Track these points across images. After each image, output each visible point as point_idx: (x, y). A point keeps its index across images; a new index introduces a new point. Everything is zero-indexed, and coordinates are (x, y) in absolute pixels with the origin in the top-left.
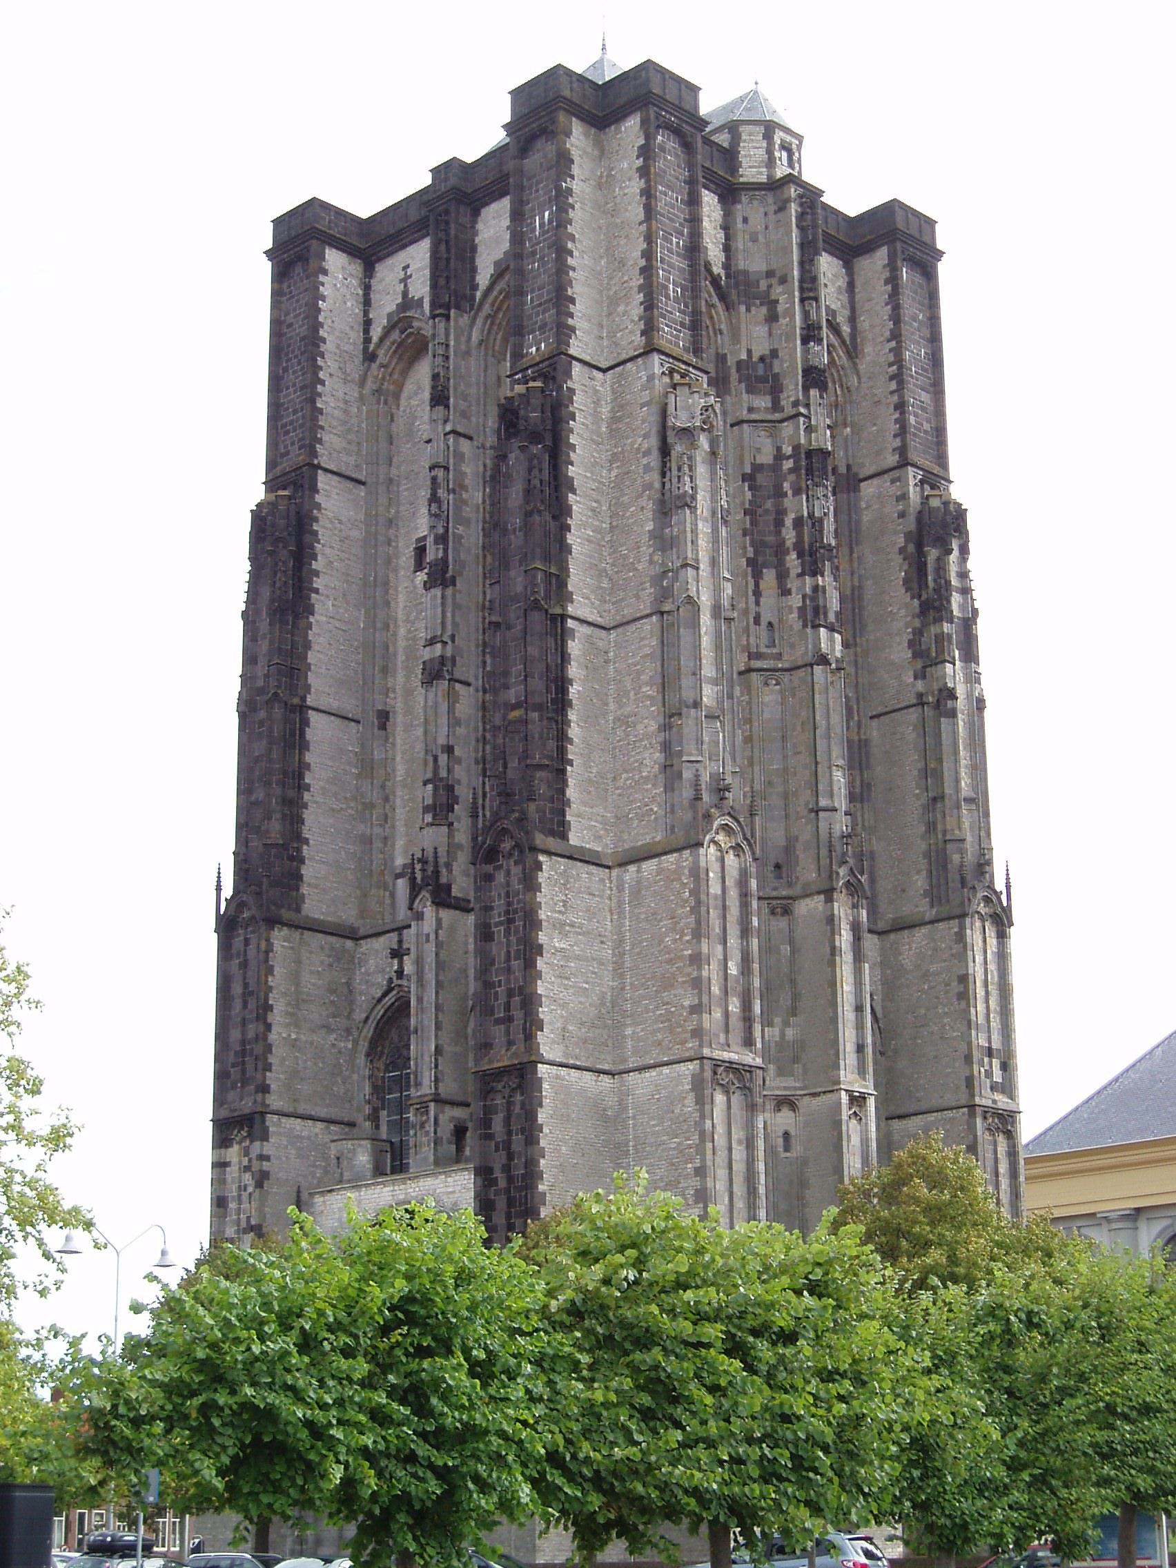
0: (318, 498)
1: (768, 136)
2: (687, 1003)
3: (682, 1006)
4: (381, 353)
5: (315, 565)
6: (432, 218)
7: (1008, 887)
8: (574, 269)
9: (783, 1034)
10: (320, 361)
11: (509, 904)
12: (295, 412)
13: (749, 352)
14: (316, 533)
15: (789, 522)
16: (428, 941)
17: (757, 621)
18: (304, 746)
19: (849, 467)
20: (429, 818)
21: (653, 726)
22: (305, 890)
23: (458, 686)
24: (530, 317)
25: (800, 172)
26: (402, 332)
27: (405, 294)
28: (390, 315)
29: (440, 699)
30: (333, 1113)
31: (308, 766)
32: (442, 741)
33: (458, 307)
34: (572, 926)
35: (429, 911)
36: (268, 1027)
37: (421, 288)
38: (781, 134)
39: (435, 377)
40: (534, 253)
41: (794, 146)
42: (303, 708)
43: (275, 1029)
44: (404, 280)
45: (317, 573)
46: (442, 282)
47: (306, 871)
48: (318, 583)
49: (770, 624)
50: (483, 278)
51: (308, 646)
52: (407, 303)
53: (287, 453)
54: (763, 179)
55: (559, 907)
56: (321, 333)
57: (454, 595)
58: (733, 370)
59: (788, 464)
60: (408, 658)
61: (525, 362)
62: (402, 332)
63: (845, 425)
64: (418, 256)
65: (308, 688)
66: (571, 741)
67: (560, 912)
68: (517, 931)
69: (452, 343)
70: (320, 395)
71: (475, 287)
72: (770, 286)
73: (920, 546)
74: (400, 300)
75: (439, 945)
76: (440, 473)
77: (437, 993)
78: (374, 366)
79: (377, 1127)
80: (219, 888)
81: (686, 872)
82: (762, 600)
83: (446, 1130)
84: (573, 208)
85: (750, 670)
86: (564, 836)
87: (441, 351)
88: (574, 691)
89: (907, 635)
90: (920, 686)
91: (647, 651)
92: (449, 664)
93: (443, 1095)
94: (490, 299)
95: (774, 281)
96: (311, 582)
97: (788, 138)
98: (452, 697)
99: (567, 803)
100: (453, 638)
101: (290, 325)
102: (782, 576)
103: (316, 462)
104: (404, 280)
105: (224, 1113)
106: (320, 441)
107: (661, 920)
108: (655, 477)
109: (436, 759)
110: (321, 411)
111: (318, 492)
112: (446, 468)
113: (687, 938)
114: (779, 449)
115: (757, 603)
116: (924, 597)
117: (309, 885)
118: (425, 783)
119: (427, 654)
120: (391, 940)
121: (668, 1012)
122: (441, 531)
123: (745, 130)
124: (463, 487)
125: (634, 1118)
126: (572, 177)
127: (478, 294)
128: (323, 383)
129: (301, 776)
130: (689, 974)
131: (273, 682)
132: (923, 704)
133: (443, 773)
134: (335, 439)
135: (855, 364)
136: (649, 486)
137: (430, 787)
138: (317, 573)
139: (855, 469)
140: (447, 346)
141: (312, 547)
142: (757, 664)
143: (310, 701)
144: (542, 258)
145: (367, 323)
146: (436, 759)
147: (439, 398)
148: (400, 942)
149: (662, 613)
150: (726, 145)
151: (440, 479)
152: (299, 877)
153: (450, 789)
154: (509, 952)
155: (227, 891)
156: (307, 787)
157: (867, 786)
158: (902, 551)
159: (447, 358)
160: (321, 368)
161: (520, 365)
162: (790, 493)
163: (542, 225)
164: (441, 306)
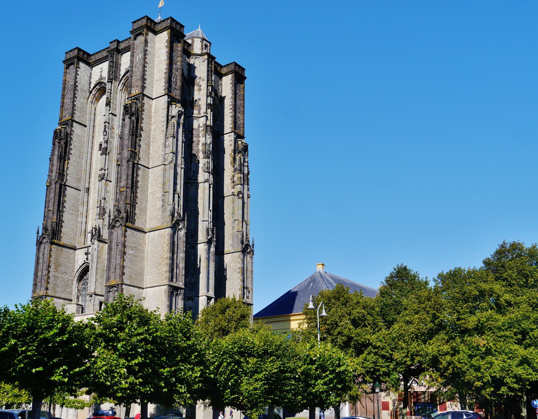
0: (73, 129)
1: (202, 42)
2: (164, 270)
4: (93, 91)
6: (109, 55)
7: (253, 245)
9: (191, 280)
11: (117, 240)
12: (68, 105)
14: (72, 138)
15: (200, 144)
16: (95, 250)
17: (190, 170)
18: (65, 196)
20: (98, 217)
22: (62, 235)
23: (108, 182)
24: (134, 83)
25: (210, 52)
27: (101, 76)
28: (96, 81)
29: (103, 185)
30: (66, 297)
31: (65, 201)
32: (103, 196)
33: (115, 80)
35: (96, 242)
36: (49, 272)
37: (105, 74)
39: (107, 98)
40: (136, 66)
42: (65, 185)
44: (101, 72)
45: (71, 149)
46: (111, 72)
47: (63, 230)
48: (71, 152)
49: (194, 171)
50: (122, 73)
51: (67, 168)
52: (101, 78)
53: (65, 116)
54: (200, 53)
57: (109, 157)
58: (188, 103)
59: (201, 129)
61: (132, 95)
64: (105, 65)
65: (67, 180)
66: (137, 198)
68: (119, 248)
69: (112, 89)
70: (75, 101)
71: (120, 75)
72: (200, 81)
73: (235, 153)
74: (99, 77)
75: (98, 251)
76: (107, 124)
77: (97, 265)
78: (91, 95)
79: (78, 301)
80: (38, 233)
81: (167, 234)
82: (192, 164)
83: (97, 303)
84: (147, 55)
86: (134, 223)
87: (110, 91)
88: (139, 184)
89: (231, 176)
90: (233, 190)
91: (160, 175)
92: (106, 176)
93: (97, 293)
94: (124, 78)
95: (201, 80)
96: (69, 151)
98: (106, 185)
99: (135, 214)
100: (108, 168)
101: (68, 82)
104: (101, 72)
105: (35, 295)
106: (75, 113)
108: (165, 128)
109: (101, 201)
110: (75, 105)
111: (73, 127)
112: (109, 123)
114: (199, 125)
115: (191, 165)
116: (235, 167)
118: (97, 207)
119: (100, 173)
120: (85, 250)
121: (159, 272)
122: (106, 140)
123: (195, 39)
124: (113, 128)
125: (148, 300)
126: (148, 47)
127: (121, 77)
128: (76, 98)
129: (63, 204)
131: (57, 178)
132: (233, 195)
133: (102, 205)
134: (79, 113)
136: (162, 131)
137: (99, 208)
138: (71, 149)
140: (111, 90)
141: (70, 142)
142: (190, 181)
143: (67, 184)
144: (138, 68)
145: (90, 83)
146: (101, 201)
147: (108, 104)
148: (88, 250)
150: (190, 43)
151: (107, 126)
152: (61, 232)
153: (104, 209)
154: (116, 254)
155: (40, 234)
156: (65, 207)
158: (230, 155)
159: (111, 93)
161: (130, 96)
162: (201, 136)
163: (139, 59)
164: (110, 79)
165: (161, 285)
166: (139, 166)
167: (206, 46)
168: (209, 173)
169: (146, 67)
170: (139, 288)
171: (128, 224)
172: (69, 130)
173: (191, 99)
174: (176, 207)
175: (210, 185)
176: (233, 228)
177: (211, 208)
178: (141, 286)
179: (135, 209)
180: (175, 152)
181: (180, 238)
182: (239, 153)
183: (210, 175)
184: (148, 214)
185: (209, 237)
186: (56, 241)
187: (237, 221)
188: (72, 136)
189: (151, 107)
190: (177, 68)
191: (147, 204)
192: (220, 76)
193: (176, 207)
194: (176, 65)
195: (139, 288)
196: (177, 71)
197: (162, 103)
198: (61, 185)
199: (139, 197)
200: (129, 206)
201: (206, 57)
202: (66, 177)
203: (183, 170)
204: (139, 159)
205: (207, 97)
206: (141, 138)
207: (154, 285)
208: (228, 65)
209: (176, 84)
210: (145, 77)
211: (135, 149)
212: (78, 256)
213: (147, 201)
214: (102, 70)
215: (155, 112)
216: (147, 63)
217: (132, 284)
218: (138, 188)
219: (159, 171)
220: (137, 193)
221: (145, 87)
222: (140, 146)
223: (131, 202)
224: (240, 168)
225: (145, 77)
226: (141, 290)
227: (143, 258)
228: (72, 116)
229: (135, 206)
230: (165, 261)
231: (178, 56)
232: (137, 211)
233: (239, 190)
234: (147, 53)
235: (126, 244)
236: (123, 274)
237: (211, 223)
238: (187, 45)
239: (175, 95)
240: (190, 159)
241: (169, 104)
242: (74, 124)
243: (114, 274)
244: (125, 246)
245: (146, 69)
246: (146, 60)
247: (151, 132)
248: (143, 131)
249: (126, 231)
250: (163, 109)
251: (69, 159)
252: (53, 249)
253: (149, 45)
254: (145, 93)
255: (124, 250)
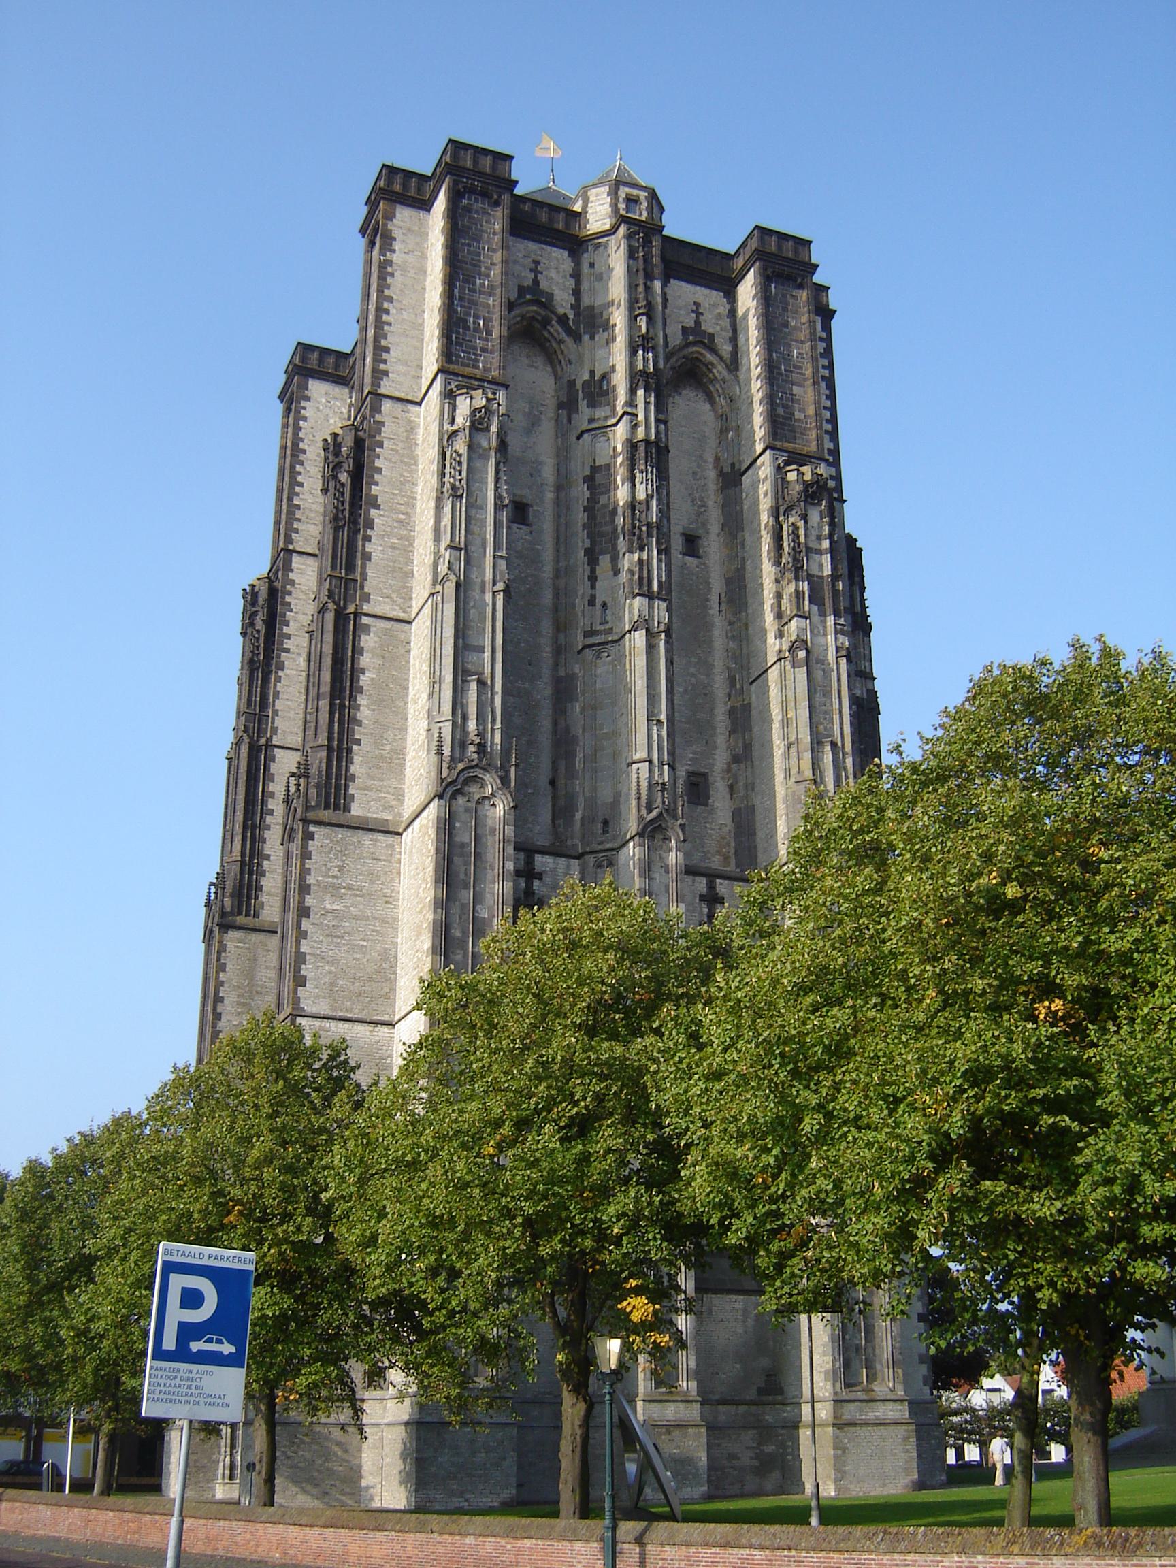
0: (291, 576)
1: (614, 193)
5: (286, 629)
8: (390, 324)
10: (298, 468)
13: (592, 373)
14: (289, 604)
17: (592, 602)
19: (733, 465)
34: (349, 888)
38: (627, 189)
41: (642, 198)
42: (269, 746)
43: (224, 1018)
45: (288, 636)
48: (288, 644)
49: (604, 604)
51: (277, 695)
55: (335, 872)
56: (301, 446)
59: (620, 460)
63: (727, 430)
66: (359, 723)
67: (334, 877)
73: (777, 517)
84: (392, 275)
85: (584, 647)
86: (347, 809)
88: (364, 680)
97: (635, 192)
102: (615, 559)
103: (291, 547)
111: (292, 571)
115: (593, 587)
117: (269, 894)
126: (394, 251)
135: (737, 377)
138: (288, 636)
139: (737, 467)
152: (259, 888)
157: (748, 747)
160: (300, 473)
166: (365, 620)
167: (632, 201)
168: (650, 596)
169: (387, 312)
170: (377, 1023)
171: (311, 815)
172: (278, 585)
173: (586, 377)
174: (472, 725)
175: (650, 634)
176: (788, 772)
177: (663, 717)
178: (386, 1018)
179: (350, 761)
180: (462, 545)
181: (493, 831)
182: (789, 509)
183: (651, 607)
184: (408, 771)
185: (655, 813)
186: (240, 920)
187: (793, 750)
188: (288, 599)
189: (411, 428)
190: (492, 287)
191: (404, 740)
192: (729, 287)
193: (472, 725)
194: (488, 276)
195: (377, 1023)
196: (490, 294)
198: (254, 750)
199: (365, 721)
200: (324, 754)
201: (622, 230)
202: (273, 722)
203: (500, 597)
204: (366, 598)
205: (633, 352)
206: (369, 532)
208: (744, 245)
209: (489, 333)
210: (383, 342)
211: (350, 567)
213: (404, 729)
215: (424, 440)
216: (390, 299)
217: (339, 1014)
218: (361, 690)
220: (358, 708)
221: (386, 373)
222: (367, 557)
223: (330, 738)
224: (795, 560)
225: (383, 342)
226: (385, 1029)
227: (390, 923)
228: (288, 539)
229: (349, 750)
231: (494, 251)
232: (353, 769)
233: (793, 638)
234: (389, 269)
235: (311, 880)
236: (301, 981)
237: (666, 767)
238: (562, 215)
239: (485, 369)
240: (588, 568)
241: (449, 396)
242: (296, 559)
244: (304, 889)
245: (385, 318)
246: (386, 292)
247: (414, 506)
248: (377, 507)
249: (309, 836)
251: (281, 667)
252: (230, 946)
253: (397, 246)
254: (382, 391)
255: (301, 901)
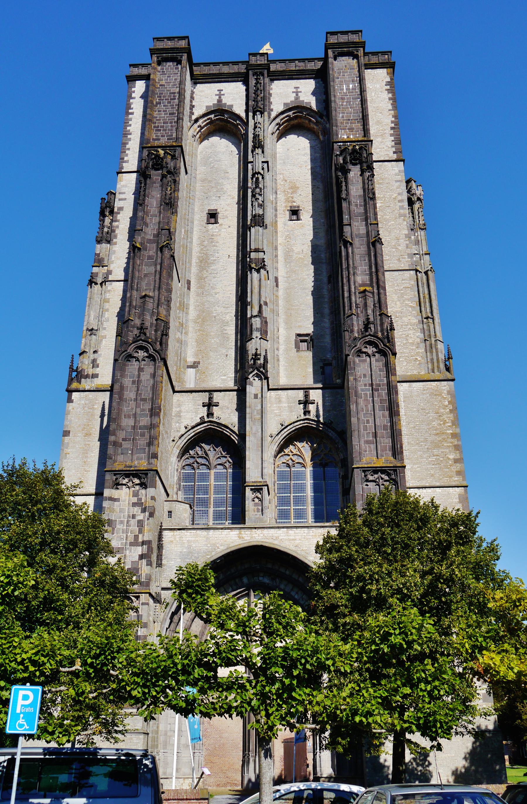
2: (452, 457)
3: (449, 459)
4: (201, 121)
21: (415, 321)
26: (215, 116)
60: (201, 262)
62: (215, 116)
78: (196, 125)
81: (445, 392)
107: (428, 413)
113: (449, 424)
130: (452, 443)
149: (417, 271)
165: (447, 484)
197: (394, 172)
207: (427, 485)
212: (179, 406)
214: (222, 93)
219: (403, 280)
230: (449, 440)
243: (373, 446)
250: (397, 181)
